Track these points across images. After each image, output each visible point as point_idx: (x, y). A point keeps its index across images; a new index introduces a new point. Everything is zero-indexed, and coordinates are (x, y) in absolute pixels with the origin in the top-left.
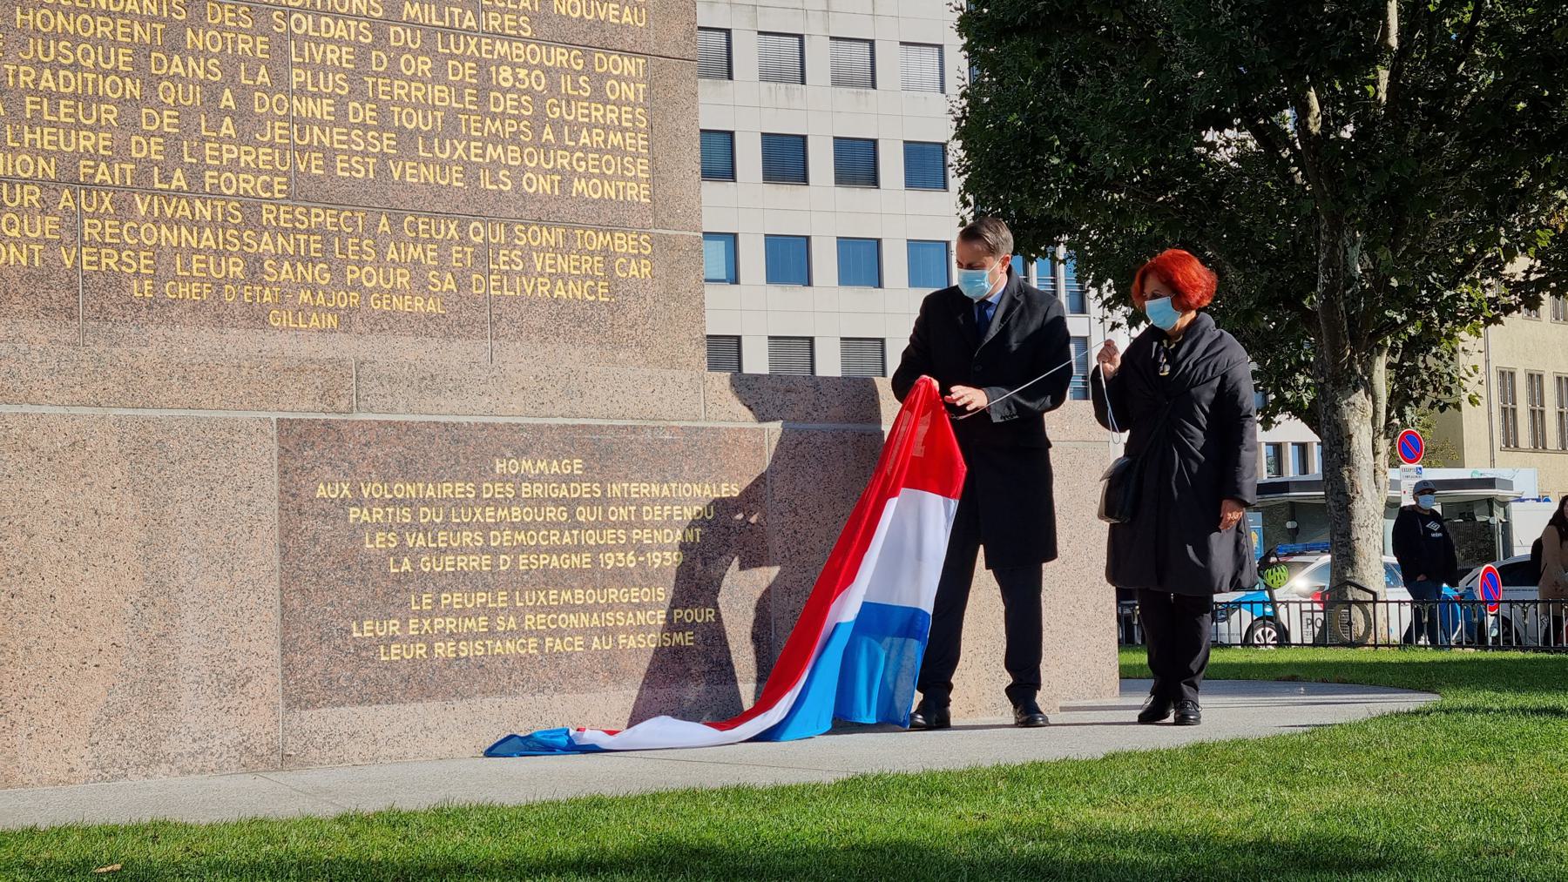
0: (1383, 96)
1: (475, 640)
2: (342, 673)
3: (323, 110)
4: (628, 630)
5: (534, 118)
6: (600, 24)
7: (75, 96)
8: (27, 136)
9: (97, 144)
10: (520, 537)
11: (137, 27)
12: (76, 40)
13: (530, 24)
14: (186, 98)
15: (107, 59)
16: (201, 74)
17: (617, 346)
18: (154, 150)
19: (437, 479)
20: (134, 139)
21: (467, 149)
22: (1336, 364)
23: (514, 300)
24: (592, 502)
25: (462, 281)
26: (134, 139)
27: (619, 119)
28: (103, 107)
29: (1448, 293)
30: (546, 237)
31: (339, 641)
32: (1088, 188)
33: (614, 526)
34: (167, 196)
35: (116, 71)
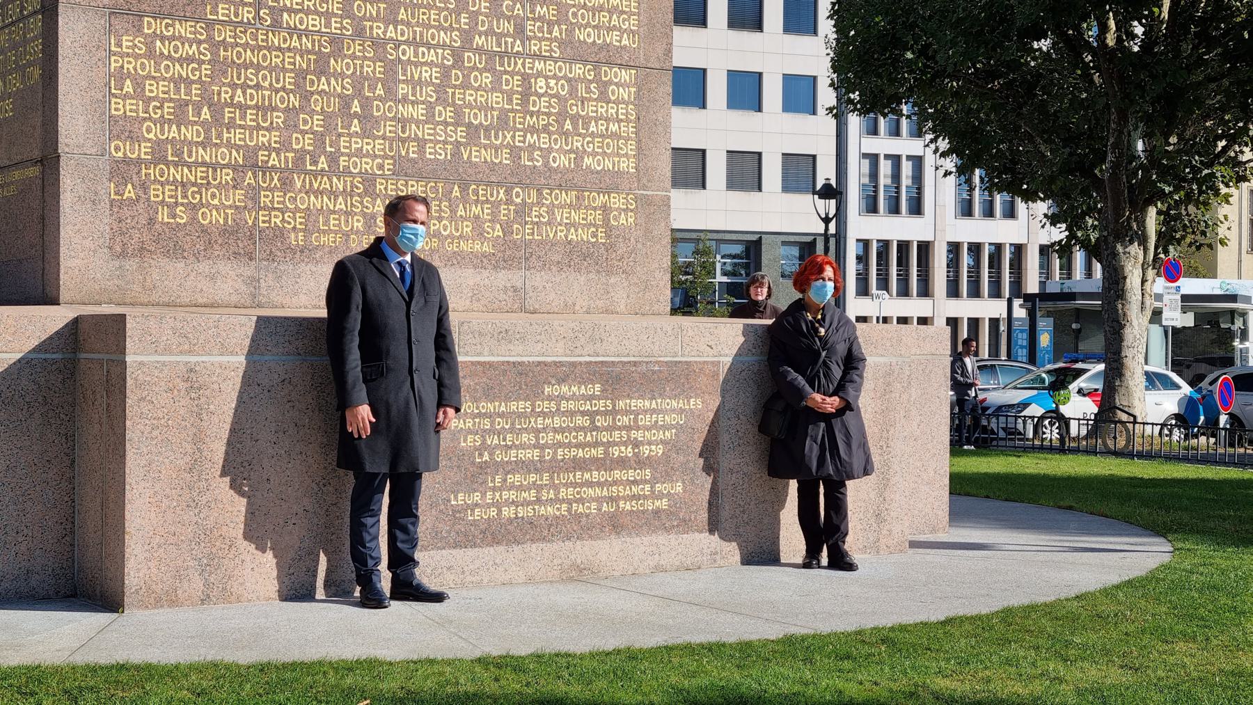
0: (1165, 14)
1: (528, 505)
3: (419, 112)
4: (626, 498)
5: (559, 114)
6: (606, 46)
7: (257, 107)
8: (226, 135)
9: (270, 139)
10: (559, 437)
11: (298, 58)
12: (258, 68)
13: (559, 47)
14: (329, 107)
15: (278, 81)
16: (339, 89)
17: (609, 273)
18: (307, 143)
19: (507, 399)
20: (295, 135)
21: (513, 137)
22: (1117, 221)
23: (541, 242)
24: (606, 413)
25: (507, 231)
26: (295, 135)
27: (617, 113)
28: (275, 114)
29: (1206, 172)
30: (567, 197)
31: (442, 507)
32: (934, 77)
33: (620, 429)
34: (315, 174)
35: (283, 89)
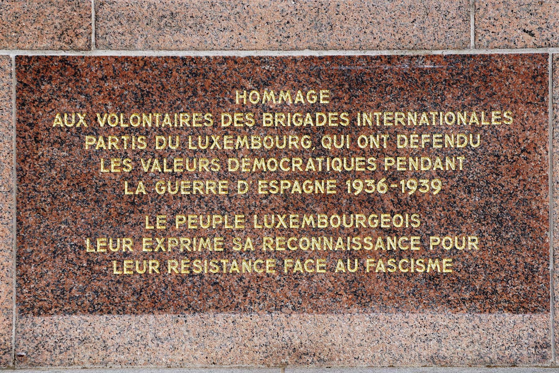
1: (210, 258)
2: (75, 285)
19: (174, 109)
31: (72, 256)
33: (363, 153)
